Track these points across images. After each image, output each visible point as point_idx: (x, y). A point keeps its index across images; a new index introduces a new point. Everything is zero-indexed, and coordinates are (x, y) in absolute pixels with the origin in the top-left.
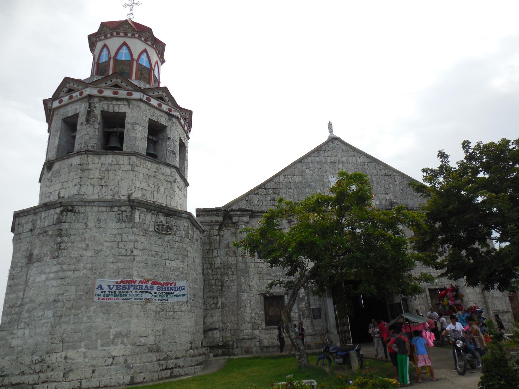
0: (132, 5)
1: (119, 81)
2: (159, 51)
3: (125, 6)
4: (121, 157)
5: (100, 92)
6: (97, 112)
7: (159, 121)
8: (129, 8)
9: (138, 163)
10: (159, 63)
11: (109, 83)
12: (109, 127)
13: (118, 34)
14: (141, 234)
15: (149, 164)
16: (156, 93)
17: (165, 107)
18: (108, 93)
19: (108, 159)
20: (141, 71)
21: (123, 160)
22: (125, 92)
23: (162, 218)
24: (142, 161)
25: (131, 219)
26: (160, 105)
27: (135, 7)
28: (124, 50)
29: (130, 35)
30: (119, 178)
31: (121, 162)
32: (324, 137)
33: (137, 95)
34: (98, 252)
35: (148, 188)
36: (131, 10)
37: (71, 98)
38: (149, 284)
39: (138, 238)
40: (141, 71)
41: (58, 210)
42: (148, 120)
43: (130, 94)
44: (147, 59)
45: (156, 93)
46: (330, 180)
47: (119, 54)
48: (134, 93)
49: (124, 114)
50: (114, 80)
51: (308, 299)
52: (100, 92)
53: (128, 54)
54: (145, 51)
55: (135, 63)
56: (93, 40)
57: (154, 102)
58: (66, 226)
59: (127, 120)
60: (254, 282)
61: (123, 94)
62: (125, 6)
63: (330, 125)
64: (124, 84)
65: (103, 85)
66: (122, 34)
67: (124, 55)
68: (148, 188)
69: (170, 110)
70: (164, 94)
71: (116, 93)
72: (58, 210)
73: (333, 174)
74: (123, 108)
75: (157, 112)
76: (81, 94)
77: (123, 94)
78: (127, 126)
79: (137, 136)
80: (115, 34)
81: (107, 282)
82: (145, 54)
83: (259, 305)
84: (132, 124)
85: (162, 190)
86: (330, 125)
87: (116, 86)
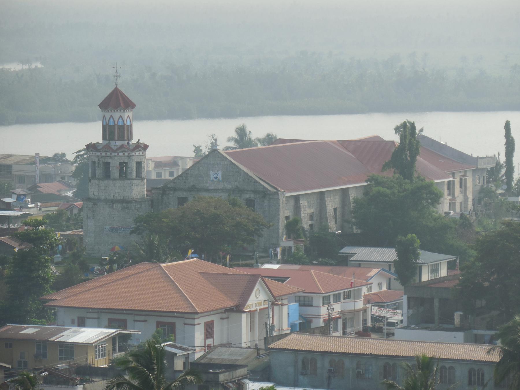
5: (101, 154)
6: (101, 162)
15: (121, 182)
17: (126, 154)
18: (104, 154)
19: (106, 182)
21: (111, 182)
23: (124, 204)
25: (113, 207)
26: (124, 154)
33: (113, 154)
34: (104, 218)
43: (111, 154)
49: (110, 163)
52: (101, 154)
57: (121, 154)
58: (94, 209)
59: (111, 165)
61: (108, 154)
69: (129, 154)
71: (106, 154)
73: (212, 170)
74: (109, 160)
77: (108, 154)
79: (115, 173)
81: (107, 227)
85: (127, 190)
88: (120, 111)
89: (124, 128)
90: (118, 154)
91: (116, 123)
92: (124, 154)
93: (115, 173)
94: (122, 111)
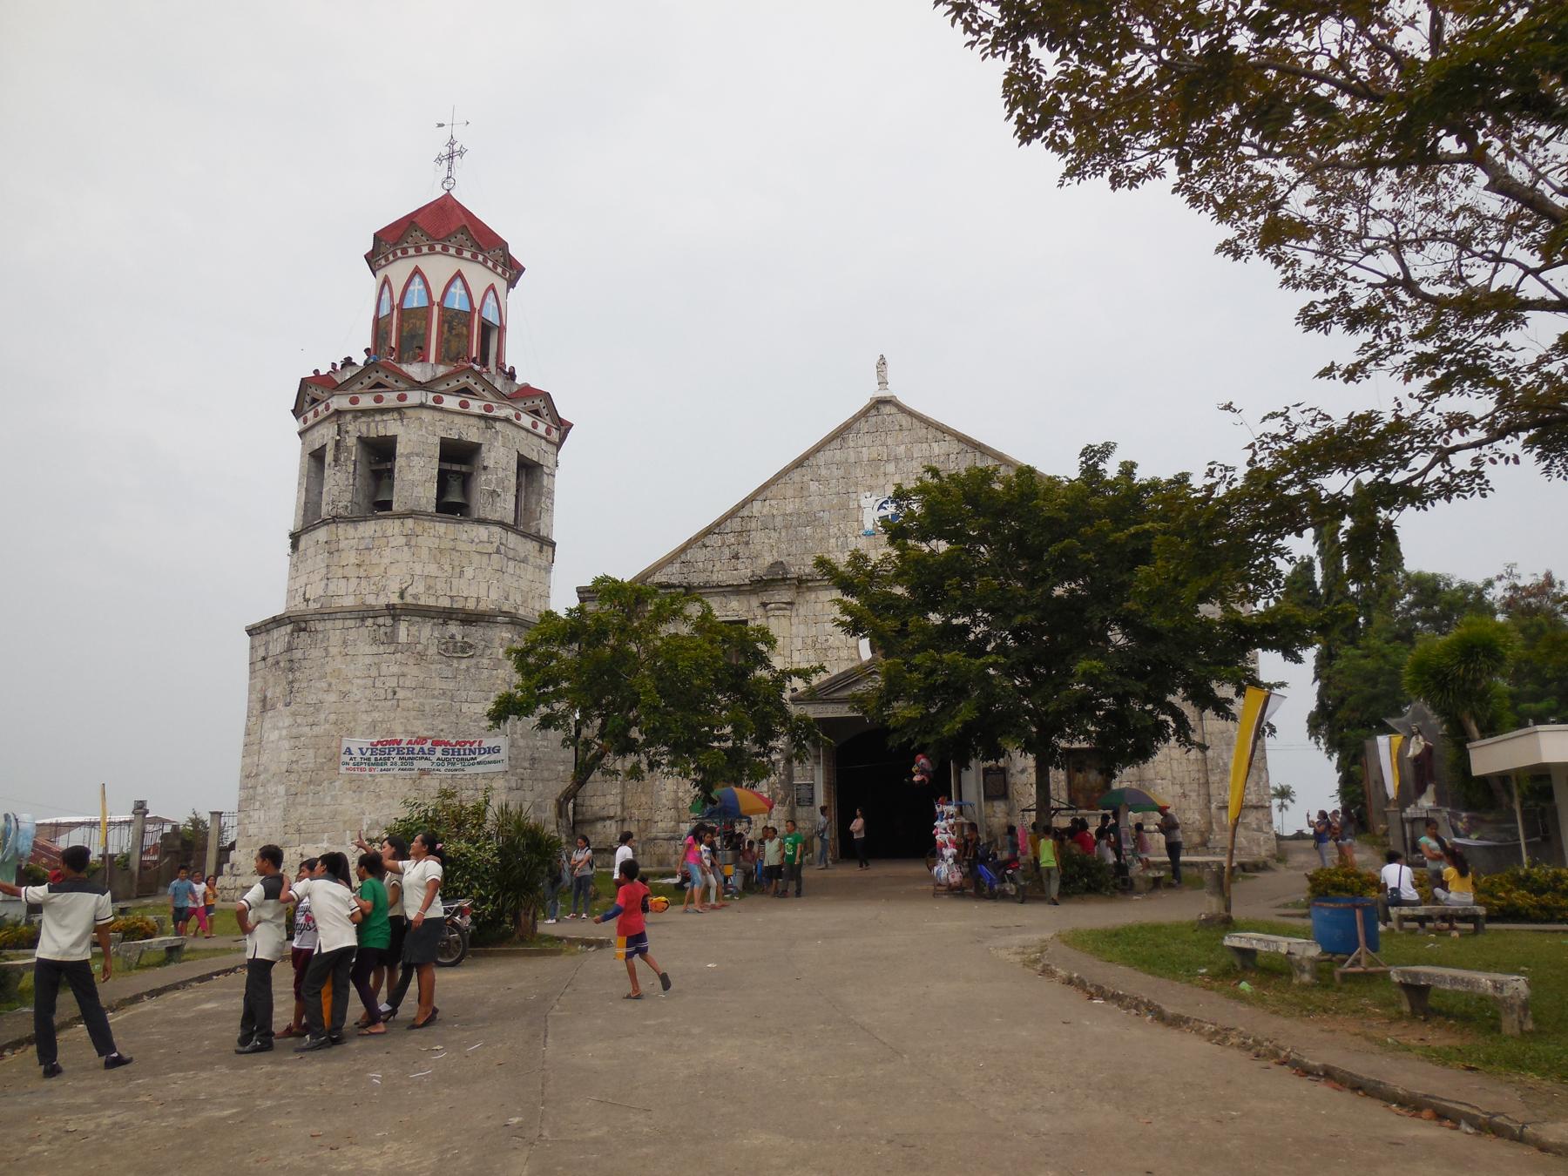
1: (382, 375)
4: (389, 522)
5: (354, 401)
6: (351, 441)
7: (464, 437)
9: (419, 530)
10: (501, 285)
11: (366, 381)
12: (378, 463)
13: (404, 251)
14: (411, 661)
15: (441, 528)
16: (453, 384)
17: (476, 406)
18: (367, 402)
19: (368, 529)
20: (450, 323)
21: (392, 527)
22: (394, 395)
23: (454, 628)
24: (427, 524)
25: (392, 638)
26: (464, 405)
28: (417, 285)
29: (425, 250)
30: (386, 561)
31: (389, 533)
33: (414, 397)
34: (345, 695)
35: (439, 574)
36: (450, 168)
38: (428, 745)
39: (405, 669)
40: (450, 323)
41: (289, 628)
42: (437, 441)
43: (402, 398)
45: (453, 384)
46: (863, 502)
47: (409, 295)
48: (409, 394)
50: (374, 375)
52: (354, 401)
53: (424, 293)
54: (459, 275)
55: (436, 309)
56: (373, 259)
57: (451, 402)
58: (298, 654)
59: (400, 449)
61: (390, 399)
62: (439, 160)
64: (391, 380)
66: (411, 251)
67: (416, 299)
68: (439, 574)
69: (488, 408)
70: (471, 381)
71: (378, 399)
72: (289, 628)
73: (871, 488)
74: (391, 427)
75: (458, 419)
76: (327, 408)
77: (390, 399)
78: (400, 462)
79: (416, 478)
81: (358, 743)
82: (459, 283)
84: (408, 456)
85: (469, 572)
87: (378, 385)
88: (459, 252)
89: (469, 326)
90: (438, 400)
91: (437, 298)
92: (464, 405)
93: (416, 478)
94: (467, 254)
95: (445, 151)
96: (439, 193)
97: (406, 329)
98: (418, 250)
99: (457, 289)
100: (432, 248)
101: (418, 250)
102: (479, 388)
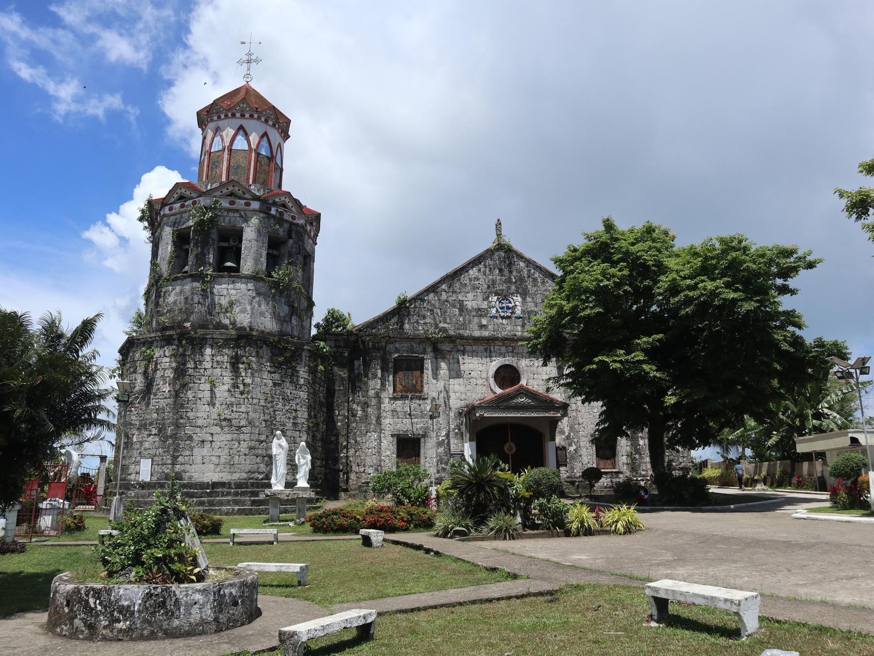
0: (249, 62)
2: (282, 130)
3: (241, 62)
8: (245, 65)
13: (234, 115)
22: (243, 202)
27: (253, 64)
32: (489, 243)
36: (249, 69)
37: (182, 206)
44: (267, 145)
47: (235, 142)
51: (449, 444)
60: (387, 421)
62: (241, 62)
63: (499, 225)
65: (218, 193)
80: (230, 115)
82: (265, 139)
83: (391, 447)
86: (499, 225)
91: (254, 146)
95: (246, 58)
96: (239, 83)
97: (232, 161)
98: (243, 116)
99: (265, 142)
100: (252, 116)
101: (243, 116)
102: (290, 205)
